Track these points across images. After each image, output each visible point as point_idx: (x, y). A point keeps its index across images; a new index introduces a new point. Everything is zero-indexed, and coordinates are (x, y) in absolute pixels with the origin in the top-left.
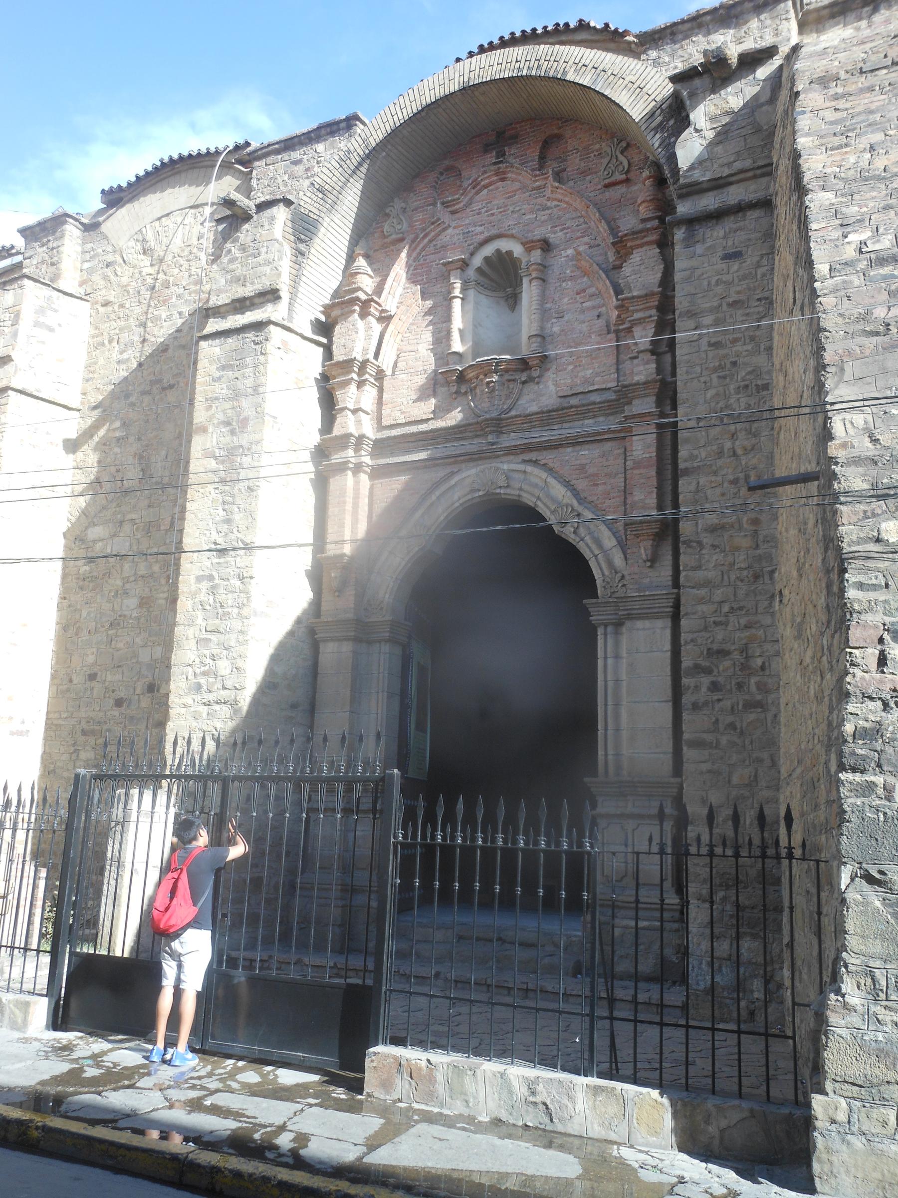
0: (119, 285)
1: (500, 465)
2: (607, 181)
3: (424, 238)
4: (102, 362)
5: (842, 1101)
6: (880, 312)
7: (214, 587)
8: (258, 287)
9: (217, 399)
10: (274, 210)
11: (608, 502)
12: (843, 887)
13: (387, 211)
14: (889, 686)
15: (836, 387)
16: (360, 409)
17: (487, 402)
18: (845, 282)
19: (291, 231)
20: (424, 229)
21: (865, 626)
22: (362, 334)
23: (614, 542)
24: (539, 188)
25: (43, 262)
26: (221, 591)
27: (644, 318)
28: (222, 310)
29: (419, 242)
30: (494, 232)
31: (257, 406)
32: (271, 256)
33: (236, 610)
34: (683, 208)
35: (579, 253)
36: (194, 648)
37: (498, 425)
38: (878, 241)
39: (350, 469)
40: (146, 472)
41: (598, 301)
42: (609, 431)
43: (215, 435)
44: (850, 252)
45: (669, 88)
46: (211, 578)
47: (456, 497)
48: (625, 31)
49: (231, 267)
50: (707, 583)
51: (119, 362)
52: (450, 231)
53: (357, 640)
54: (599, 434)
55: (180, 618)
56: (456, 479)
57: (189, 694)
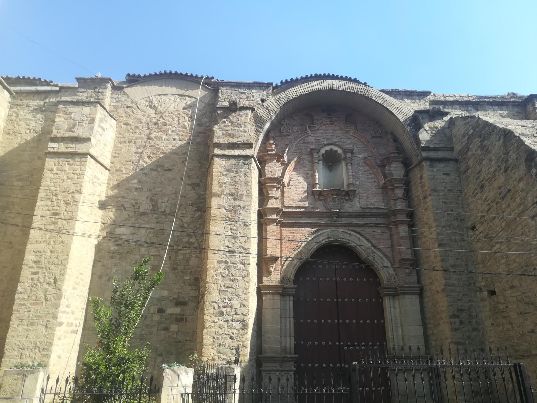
0: (135, 118)
4: (124, 150)
9: (225, 183)
11: (385, 250)
13: (282, 122)
16: (277, 198)
17: (328, 204)
23: (389, 265)
26: (232, 268)
28: (222, 145)
32: (247, 130)
33: (241, 278)
37: (339, 215)
40: (155, 204)
41: (373, 176)
43: (225, 199)
45: (411, 114)
46: (226, 262)
47: (321, 240)
49: (226, 128)
50: (453, 285)
51: (136, 153)
52: (310, 137)
53: (281, 295)
56: (321, 232)
57: (215, 316)
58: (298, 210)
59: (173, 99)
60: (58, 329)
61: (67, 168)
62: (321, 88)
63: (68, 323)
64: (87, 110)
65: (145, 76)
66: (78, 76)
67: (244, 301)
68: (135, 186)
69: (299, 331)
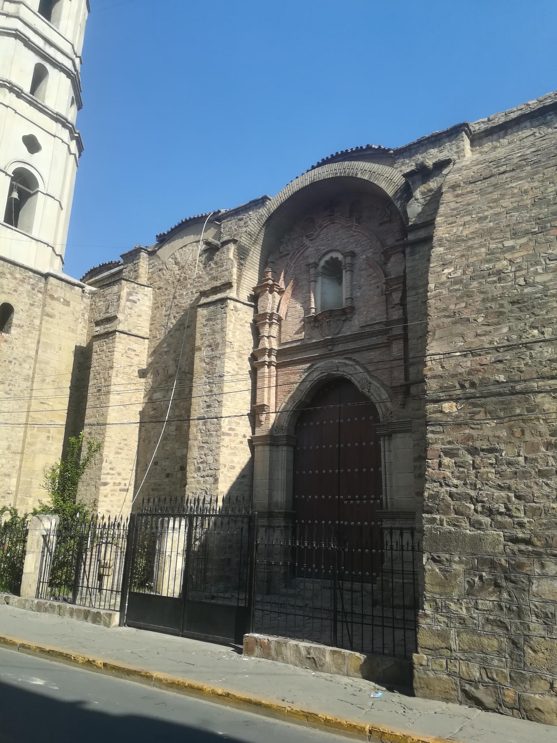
0: (165, 280)
1: (334, 360)
2: (380, 222)
3: (298, 253)
4: (158, 316)
5: (425, 656)
6: (452, 307)
7: (205, 422)
8: (223, 281)
9: (205, 334)
10: (229, 245)
12: (424, 563)
14: (442, 476)
15: (431, 342)
18: (440, 292)
19: (237, 254)
20: (297, 249)
21: (434, 450)
22: (270, 301)
23: (387, 396)
24: (349, 227)
25: (131, 270)
26: (209, 424)
27: (397, 288)
28: (207, 292)
29: (296, 255)
30: (330, 249)
31: (223, 337)
32: (228, 267)
33: (215, 433)
34: (411, 237)
35: (367, 257)
36: (197, 450)
37: (333, 342)
38: (456, 273)
39: (266, 365)
42: (383, 343)
44: (444, 278)
45: (403, 180)
47: (315, 376)
48: (389, 149)
49: (211, 272)
51: (165, 316)
52: (310, 249)
53: (271, 445)
54: (378, 344)
55: (191, 436)
57: (195, 472)
58: (295, 345)
59: (191, 248)
60: (102, 488)
61: (105, 348)
62: (301, 186)
63: (114, 483)
64: (115, 288)
65: (168, 232)
66: (121, 254)
67: (216, 456)
68: (165, 349)
69: (297, 483)
